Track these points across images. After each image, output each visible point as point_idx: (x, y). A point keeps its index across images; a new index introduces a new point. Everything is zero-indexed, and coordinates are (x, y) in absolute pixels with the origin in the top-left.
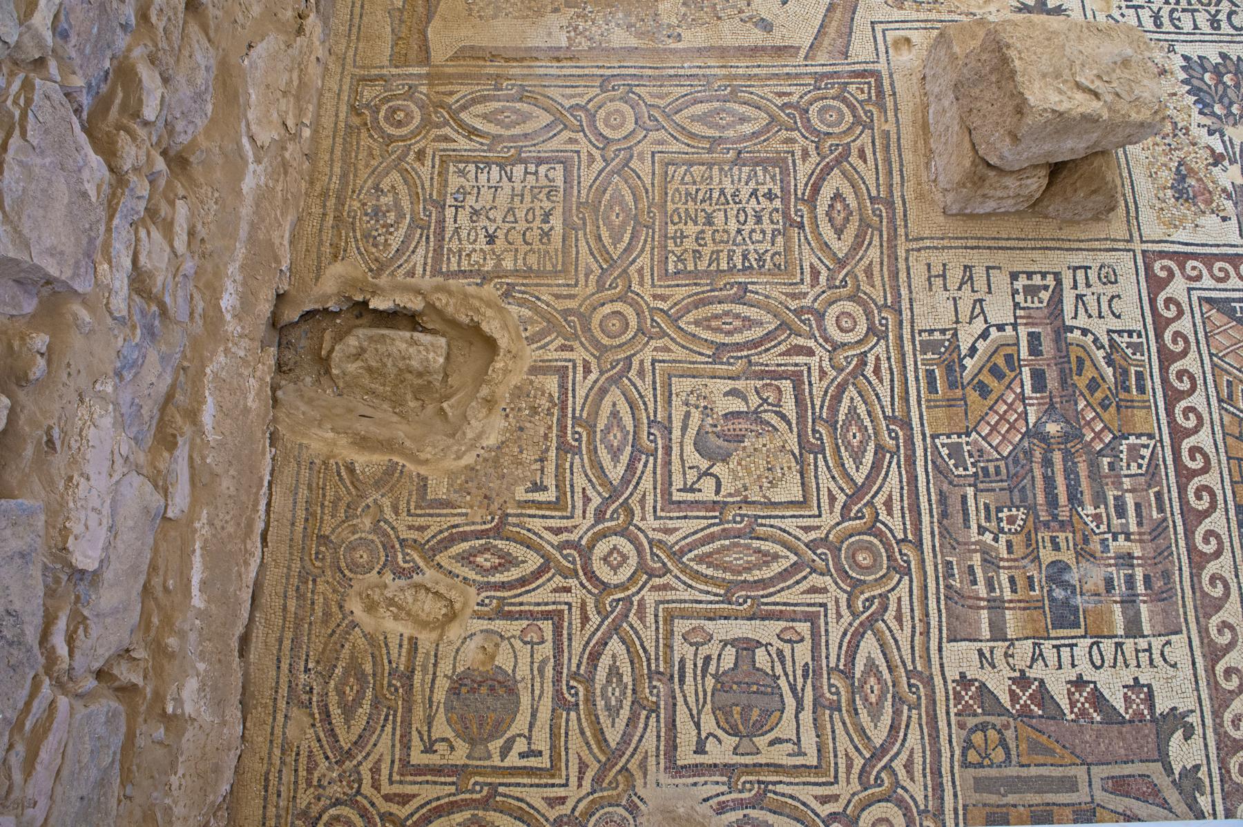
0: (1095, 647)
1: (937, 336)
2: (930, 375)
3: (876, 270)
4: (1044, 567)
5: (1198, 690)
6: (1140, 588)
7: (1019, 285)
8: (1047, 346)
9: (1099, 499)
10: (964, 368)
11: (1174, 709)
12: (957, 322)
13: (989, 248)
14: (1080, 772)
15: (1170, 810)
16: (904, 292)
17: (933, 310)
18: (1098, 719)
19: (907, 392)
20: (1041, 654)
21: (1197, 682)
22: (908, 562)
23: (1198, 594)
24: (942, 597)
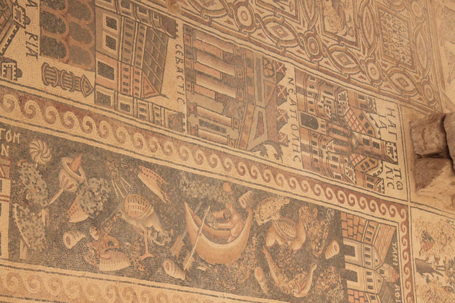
0: (297, 128)
1: (374, 106)
2: (362, 98)
3: (389, 89)
4: (316, 118)
5: (288, 167)
6: (315, 156)
7: (392, 145)
8: (376, 150)
9: (337, 152)
10: (367, 112)
11: (283, 154)
12: (379, 116)
13: (402, 137)
14: (263, 105)
15: (255, 138)
16: (385, 98)
17: (383, 106)
18: (278, 120)
19: (357, 86)
20: (293, 104)
21: (290, 168)
22: (313, 63)
23: (314, 181)
24: (306, 72)
